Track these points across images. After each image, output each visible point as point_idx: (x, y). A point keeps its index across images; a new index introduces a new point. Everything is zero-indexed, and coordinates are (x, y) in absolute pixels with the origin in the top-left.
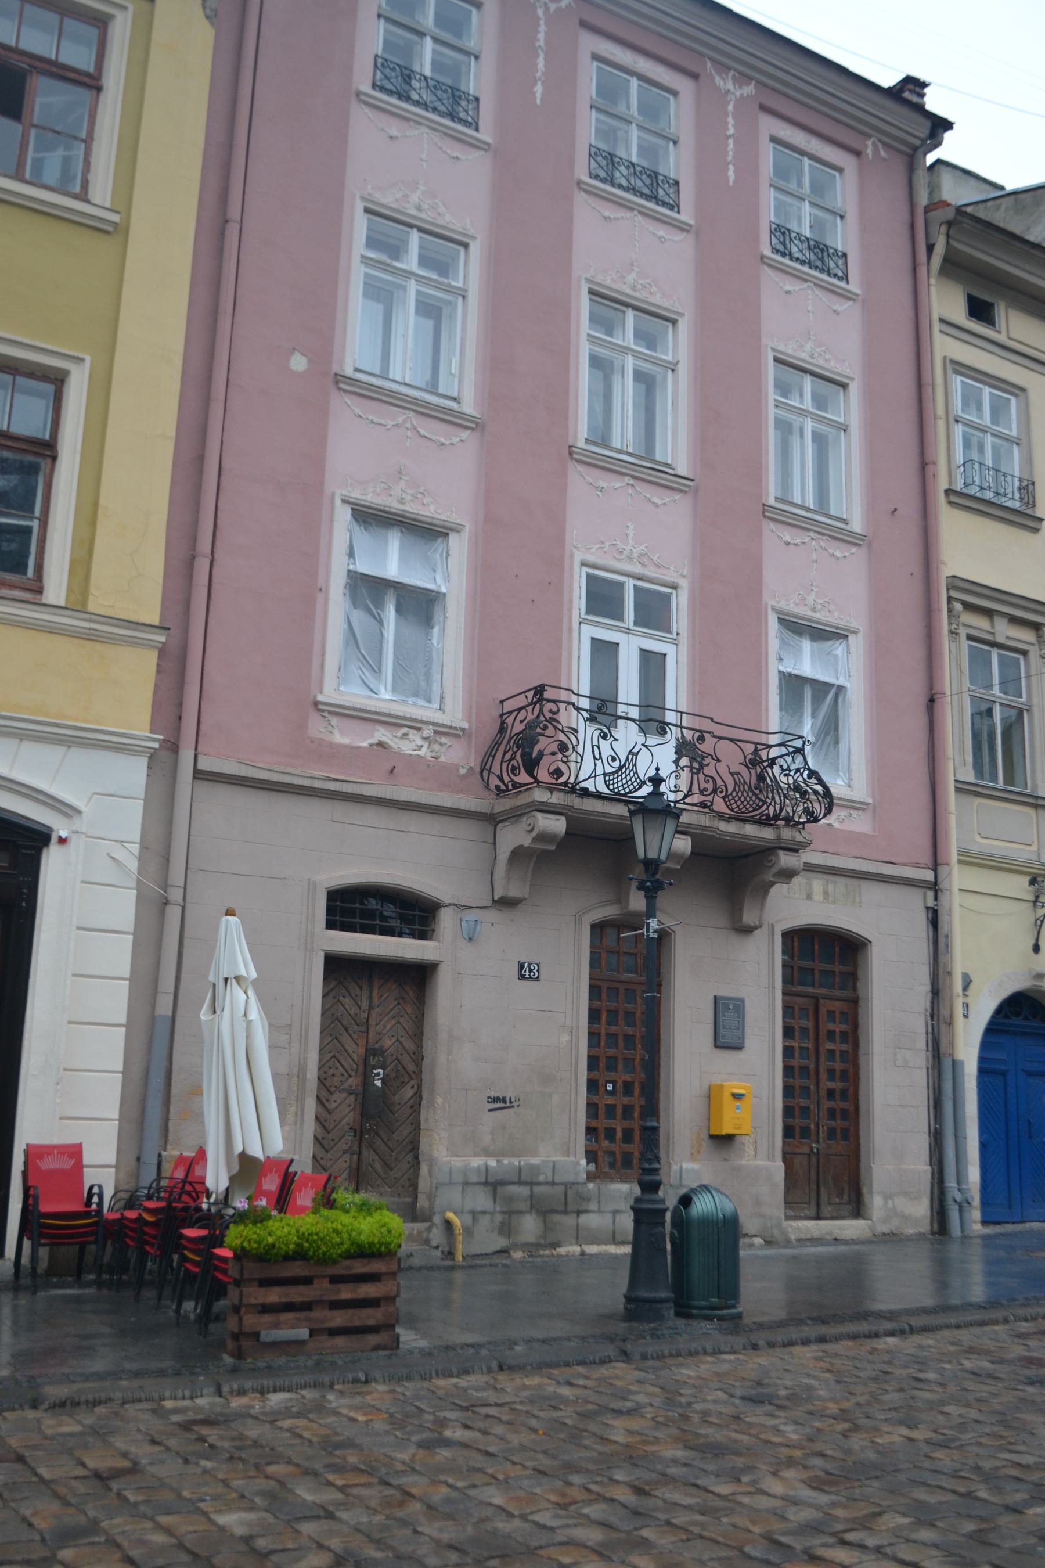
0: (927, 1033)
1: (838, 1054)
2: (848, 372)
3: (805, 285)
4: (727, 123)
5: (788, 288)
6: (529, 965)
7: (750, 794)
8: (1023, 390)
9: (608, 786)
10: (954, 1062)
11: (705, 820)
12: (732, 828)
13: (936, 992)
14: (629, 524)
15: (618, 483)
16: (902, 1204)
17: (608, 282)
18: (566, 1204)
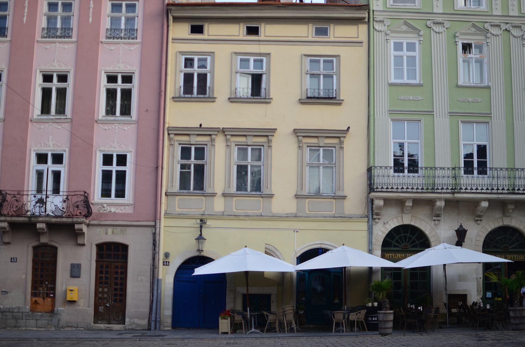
0: (151, 271)
1: (119, 278)
2: (134, 68)
3: (119, 45)
4: (90, 3)
5: (112, 48)
6: (14, 258)
7: (60, 210)
8: (213, 53)
9: (16, 214)
10: (158, 279)
11: (47, 219)
12: (58, 220)
13: (154, 259)
14: (50, 136)
15: (47, 125)
16: (136, 321)
17: (47, 68)
18: (22, 317)
